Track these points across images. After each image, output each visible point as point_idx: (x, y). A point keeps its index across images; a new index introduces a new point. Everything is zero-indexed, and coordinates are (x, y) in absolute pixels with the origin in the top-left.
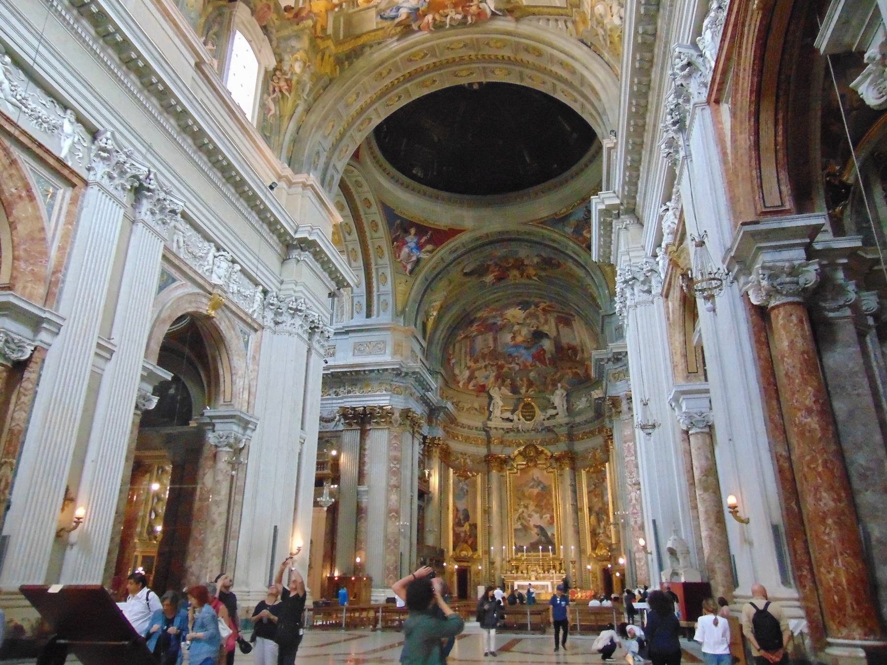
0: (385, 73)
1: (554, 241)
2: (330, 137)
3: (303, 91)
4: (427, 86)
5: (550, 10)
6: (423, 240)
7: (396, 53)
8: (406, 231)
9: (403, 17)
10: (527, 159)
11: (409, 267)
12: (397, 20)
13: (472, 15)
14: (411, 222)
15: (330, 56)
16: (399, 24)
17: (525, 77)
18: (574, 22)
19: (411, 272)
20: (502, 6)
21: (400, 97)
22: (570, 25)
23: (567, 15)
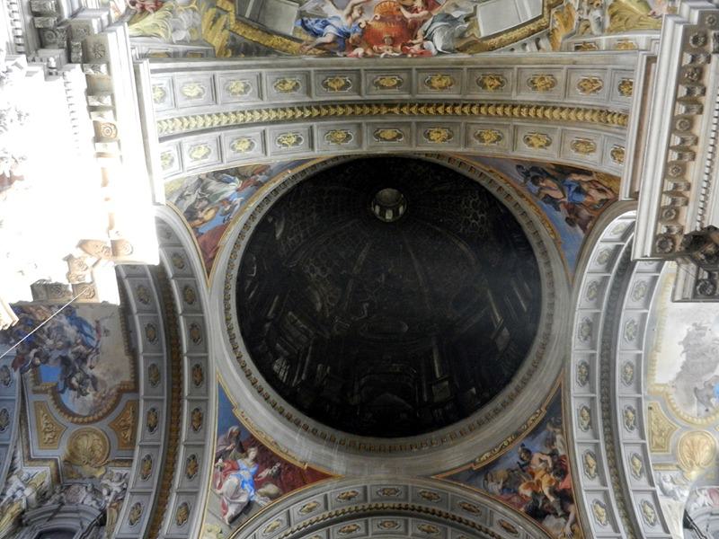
0: (288, 86)
1: (470, 509)
2: (188, 102)
3: (174, 30)
4: (336, 141)
5: (517, 33)
6: (264, 474)
7: (310, 65)
8: (243, 450)
9: (328, 39)
10: (436, 366)
11: (232, 511)
12: (320, 40)
13: (413, 54)
14: (252, 436)
15: (225, 27)
16: (321, 46)
17: (472, 138)
18: (550, 35)
19: (233, 520)
20: (452, 45)
21: (299, 140)
22: (544, 43)
23: (540, 30)
